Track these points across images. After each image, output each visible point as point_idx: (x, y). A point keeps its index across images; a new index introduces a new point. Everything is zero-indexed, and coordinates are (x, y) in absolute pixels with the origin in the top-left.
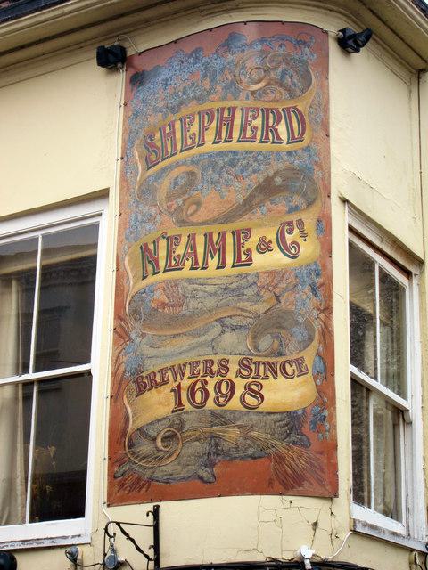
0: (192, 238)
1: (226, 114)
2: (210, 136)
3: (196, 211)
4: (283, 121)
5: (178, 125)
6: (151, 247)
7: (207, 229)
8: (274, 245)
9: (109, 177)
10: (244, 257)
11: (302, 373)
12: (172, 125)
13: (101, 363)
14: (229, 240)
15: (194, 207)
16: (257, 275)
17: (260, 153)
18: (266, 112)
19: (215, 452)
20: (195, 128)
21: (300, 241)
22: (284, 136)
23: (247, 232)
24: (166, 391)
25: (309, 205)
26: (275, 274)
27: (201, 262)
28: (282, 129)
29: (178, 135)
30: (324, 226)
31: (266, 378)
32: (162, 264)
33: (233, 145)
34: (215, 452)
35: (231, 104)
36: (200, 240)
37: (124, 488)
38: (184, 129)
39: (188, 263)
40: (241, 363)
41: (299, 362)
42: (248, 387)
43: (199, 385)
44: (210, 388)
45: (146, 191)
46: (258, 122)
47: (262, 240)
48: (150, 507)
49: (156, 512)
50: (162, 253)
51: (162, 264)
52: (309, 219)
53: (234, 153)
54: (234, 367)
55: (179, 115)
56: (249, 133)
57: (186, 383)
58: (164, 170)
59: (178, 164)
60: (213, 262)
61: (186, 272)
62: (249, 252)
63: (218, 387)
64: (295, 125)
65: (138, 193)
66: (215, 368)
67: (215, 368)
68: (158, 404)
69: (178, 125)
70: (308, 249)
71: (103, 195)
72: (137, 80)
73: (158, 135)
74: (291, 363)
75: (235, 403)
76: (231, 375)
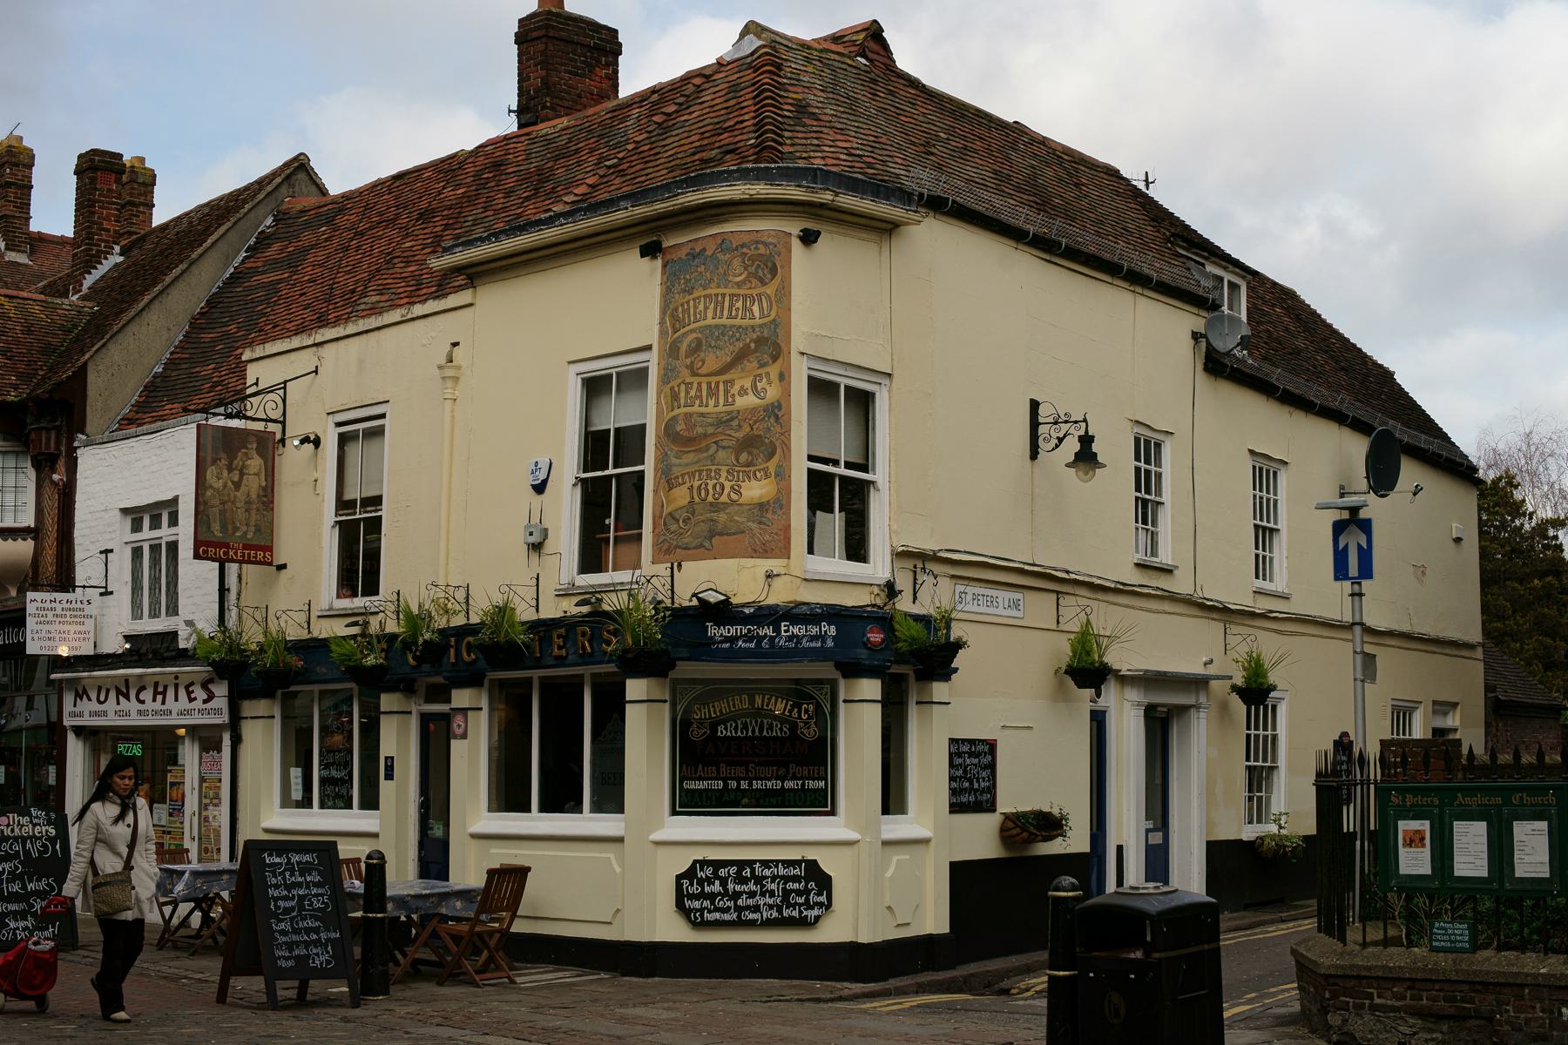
0: (700, 384)
1: (720, 298)
2: (710, 313)
4: (756, 303)
6: (676, 389)
7: (709, 379)
8: (750, 391)
9: (653, 338)
10: (730, 400)
11: (767, 476)
12: (688, 302)
13: (649, 467)
14: (721, 387)
16: (738, 411)
17: (740, 327)
18: (745, 297)
20: (701, 307)
21: (767, 387)
22: (757, 314)
23: (732, 382)
24: (684, 489)
25: (774, 362)
26: (754, 410)
28: (756, 308)
30: (784, 377)
33: (724, 321)
35: (720, 291)
36: (704, 387)
37: (664, 551)
38: (696, 308)
39: (698, 402)
40: (728, 472)
41: (766, 470)
42: (732, 487)
43: (703, 486)
44: (710, 488)
46: (740, 304)
47: (742, 387)
50: (683, 394)
51: (682, 402)
52: (773, 371)
53: (724, 326)
54: (724, 474)
55: (692, 296)
56: (734, 313)
57: (696, 484)
59: (692, 331)
60: (712, 403)
64: (765, 305)
65: (671, 351)
66: (713, 474)
67: (713, 474)
68: (681, 496)
69: (692, 303)
70: (772, 393)
71: (648, 348)
74: (759, 471)
75: (724, 498)
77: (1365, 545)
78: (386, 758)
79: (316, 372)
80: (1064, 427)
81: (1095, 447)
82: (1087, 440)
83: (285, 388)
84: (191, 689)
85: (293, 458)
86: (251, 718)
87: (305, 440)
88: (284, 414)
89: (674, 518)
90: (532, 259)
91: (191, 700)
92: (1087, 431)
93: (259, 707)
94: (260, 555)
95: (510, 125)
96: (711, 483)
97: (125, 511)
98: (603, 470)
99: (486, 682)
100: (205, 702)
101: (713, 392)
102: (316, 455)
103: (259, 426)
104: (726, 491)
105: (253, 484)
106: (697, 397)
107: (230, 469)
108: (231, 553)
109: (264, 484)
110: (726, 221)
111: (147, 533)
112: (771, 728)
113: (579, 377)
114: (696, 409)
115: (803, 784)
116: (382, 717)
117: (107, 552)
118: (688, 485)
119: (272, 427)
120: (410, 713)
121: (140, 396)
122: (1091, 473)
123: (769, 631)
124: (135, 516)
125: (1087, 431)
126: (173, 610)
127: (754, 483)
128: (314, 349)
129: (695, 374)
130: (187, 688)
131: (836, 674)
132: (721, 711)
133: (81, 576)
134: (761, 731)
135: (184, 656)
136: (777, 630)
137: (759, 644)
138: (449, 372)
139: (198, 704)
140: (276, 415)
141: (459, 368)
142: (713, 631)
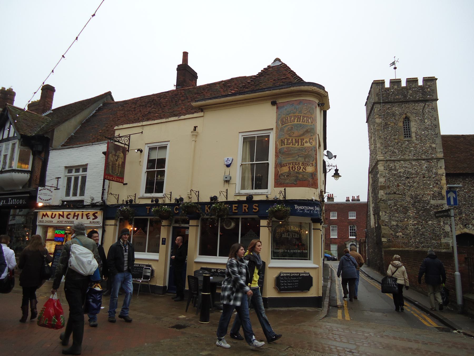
0: (292, 139)
1: (299, 117)
2: (296, 120)
3: (293, 135)
5: (289, 118)
6: (283, 140)
8: (308, 142)
9: (274, 126)
10: (303, 144)
12: (287, 118)
14: (300, 140)
15: (292, 134)
16: (305, 147)
17: (306, 125)
18: (307, 117)
19: (297, 179)
20: (293, 119)
21: (312, 142)
22: (310, 122)
27: (294, 144)
28: (310, 120)
29: (289, 120)
31: (307, 166)
32: (286, 144)
33: (300, 123)
34: (297, 179)
36: (294, 140)
37: (277, 184)
39: (291, 144)
40: (302, 163)
41: (312, 164)
42: (303, 168)
43: (294, 167)
44: (296, 167)
45: (282, 130)
46: (305, 119)
47: (306, 141)
48: (284, 188)
49: (285, 189)
50: (286, 142)
51: (286, 144)
53: (301, 124)
54: (301, 164)
56: (304, 121)
57: (291, 166)
58: (286, 126)
59: (289, 125)
60: (297, 144)
61: (291, 145)
62: (304, 143)
63: (298, 167)
65: (280, 130)
67: (297, 164)
69: (289, 118)
71: (272, 129)
72: (277, 108)
73: (284, 119)
75: (301, 170)
76: (300, 165)
77: (455, 197)
78: (163, 239)
79: (142, 133)
80: (331, 167)
81: (339, 172)
82: (337, 170)
83: (130, 137)
84: (88, 215)
85: (132, 156)
86: (110, 225)
87: (138, 150)
88: (129, 143)
89: (283, 175)
90: (227, 105)
91: (88, 218)
92: (337, 168)
93: (112, 222)
94: (121, 180)
95: (174, 88)
96: (296, 166)
97: (66, 167)
98: (252, 162)
99: (200, 219)
100: (93, 219)
101: (297, 142)
102: (141, 155)
103: (123, 145)
104: (302, 169)
105: (120, 161)
106: (291, 143)
107: (115, 156)
108: (114, 179)
109: (123, 161)
110: (301, 97)
111: (74, 174)
112: (295, 235)
113: (243, 137)
114: (291, 145)
115: (302, 251)
116: (261, 227)
117: (58, 178)
118: (288, 166)
119: (127, 147)
120: (198, 226)
121: (67, 140)
122: (338, 178)
123: (312, 208)
124: (69, 169)
125: (337, 168)
126: (82, 194)
127: (309, 167)
128: (142, 127)
129: (290, 136)
130: (87, 215)
131: (311, 222)
132: (283, 230)
133: (47, 184)
134: (293, 236)
135: (84, 207)
136: (314, 208)
137: (310, 212)
138: (195, 133)
139: (91, 220)
140: (127, 143)
141: (198, 133)
142: (296, 207)
